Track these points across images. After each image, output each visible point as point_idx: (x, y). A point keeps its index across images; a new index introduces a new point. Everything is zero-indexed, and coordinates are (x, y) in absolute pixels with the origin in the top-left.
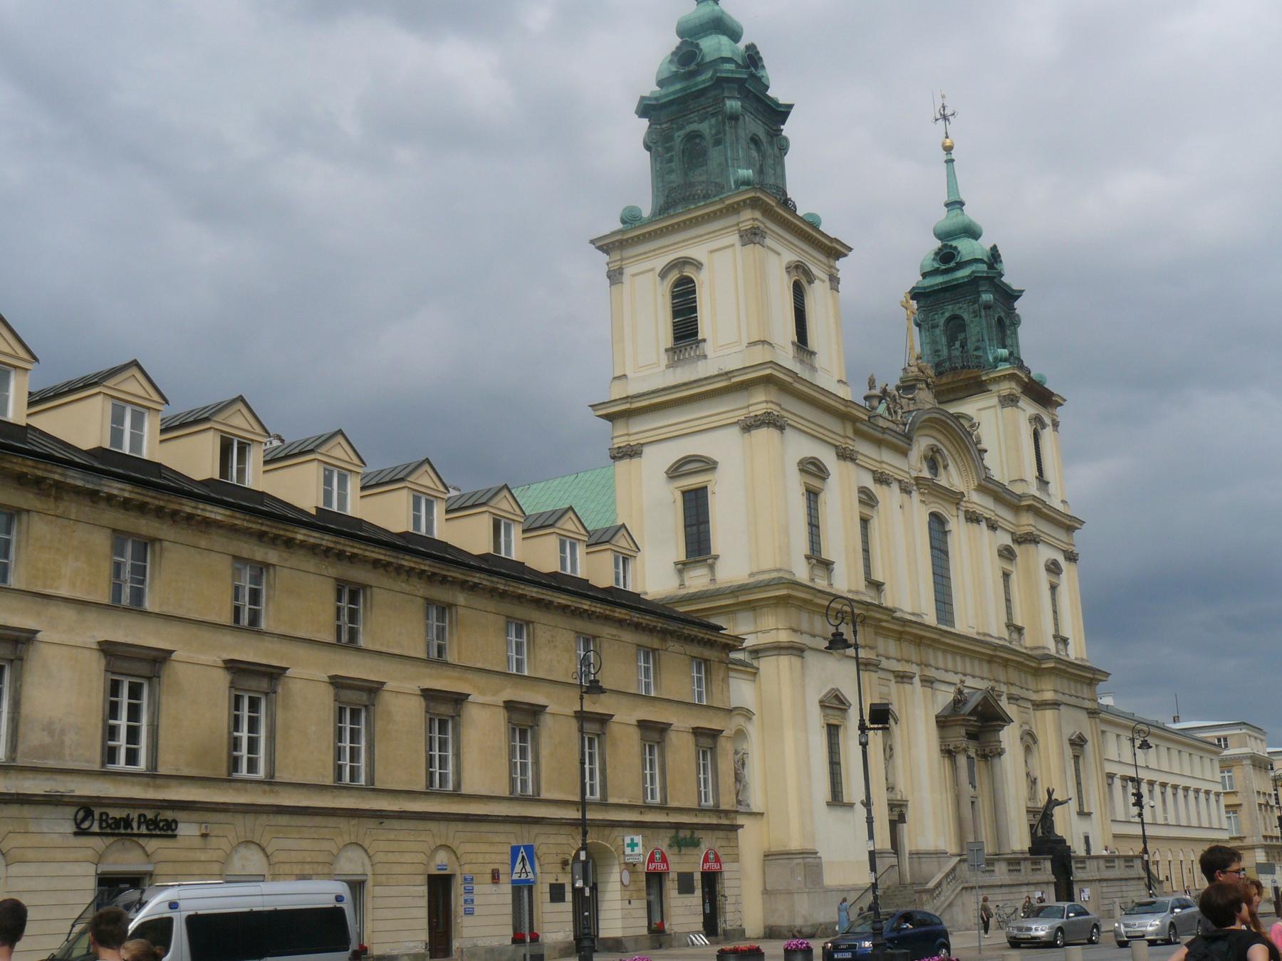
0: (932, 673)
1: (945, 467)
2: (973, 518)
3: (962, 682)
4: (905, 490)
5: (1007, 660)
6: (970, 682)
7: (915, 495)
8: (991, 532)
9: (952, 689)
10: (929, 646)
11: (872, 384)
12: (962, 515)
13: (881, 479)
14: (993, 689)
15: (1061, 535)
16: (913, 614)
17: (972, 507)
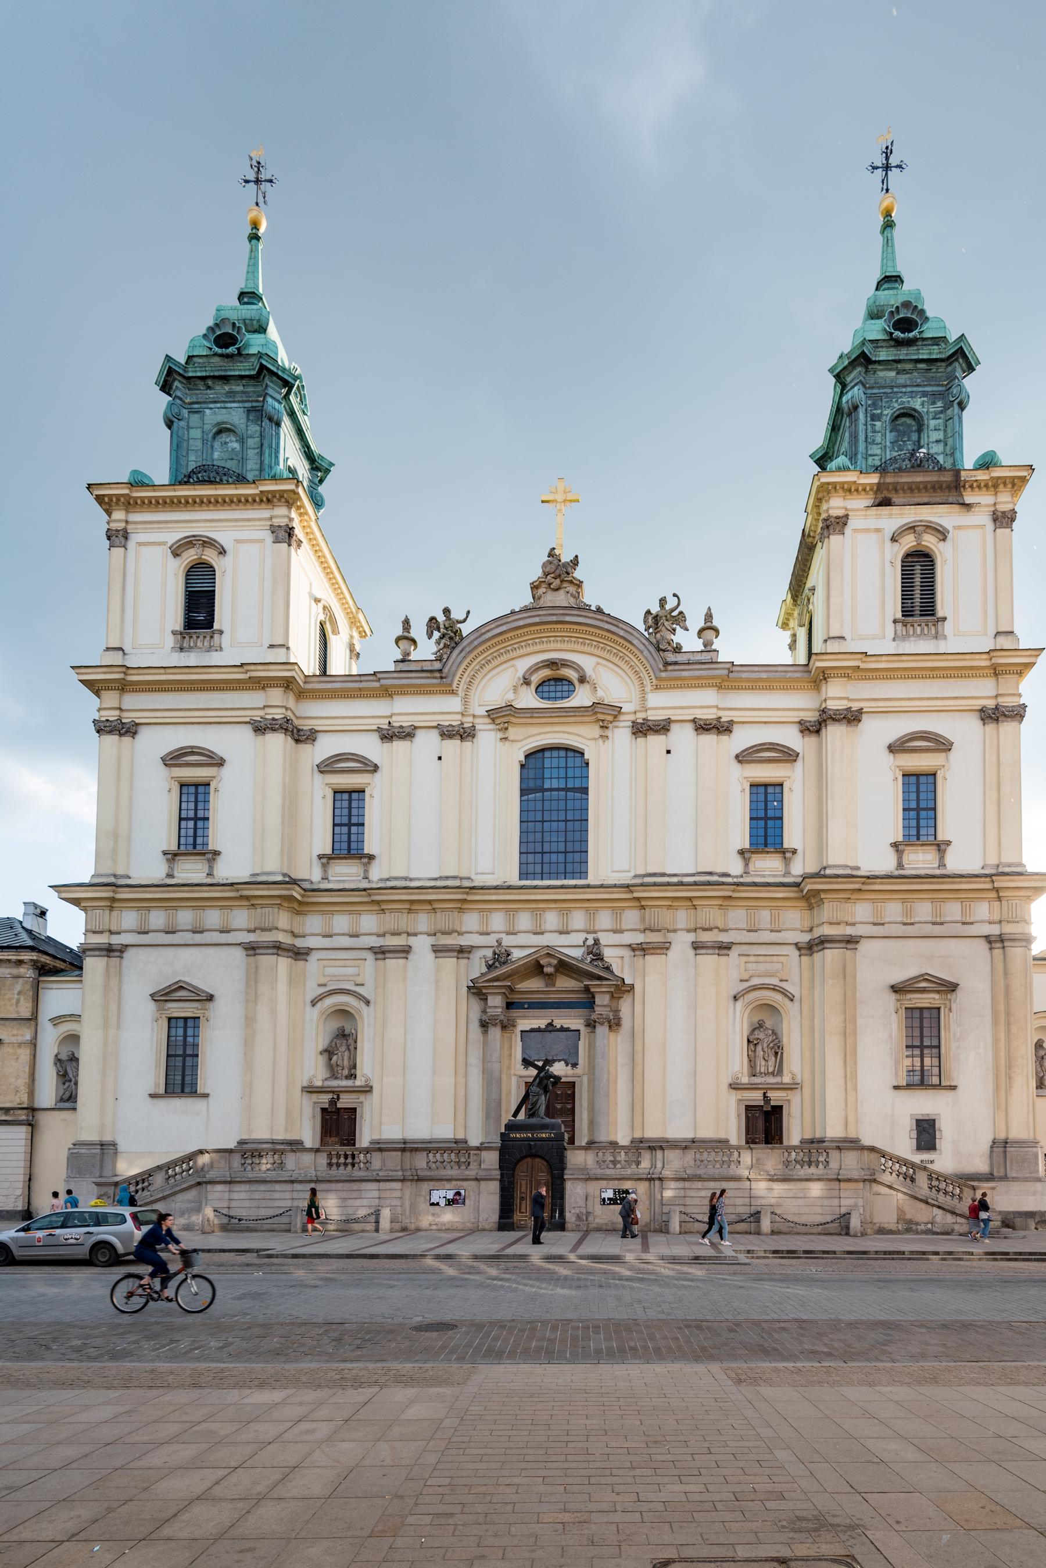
0: (465, 941)
1: (582, 680)
2: (642, 729)
3: (499, 942)
4: (447, 733)
5: (690, 899)
6: (507, 941)
7: (487, 737)
8: (709, 739)
9: (489, 953)
10: (461, 910)
11: (406, 624)
12: (621, 734)
13: (389, 735)
14: (597, 942)
15: (983, 691)
16: (440, 878)
17: (640, 717)
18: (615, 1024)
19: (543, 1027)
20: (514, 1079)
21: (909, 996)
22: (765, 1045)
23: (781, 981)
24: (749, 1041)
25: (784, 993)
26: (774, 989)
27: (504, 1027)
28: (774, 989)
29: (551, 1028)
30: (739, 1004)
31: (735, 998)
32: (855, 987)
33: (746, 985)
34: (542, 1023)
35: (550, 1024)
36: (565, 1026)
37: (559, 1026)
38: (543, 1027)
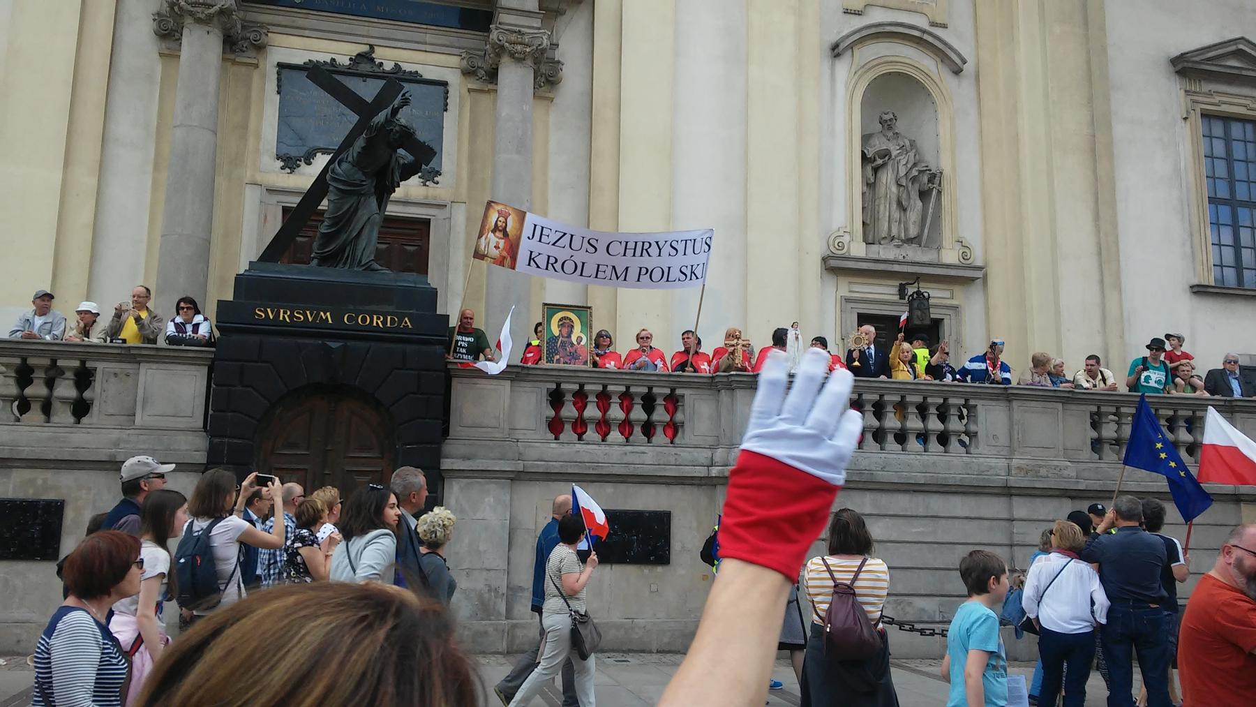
18: (547, 77)
19: (344, 61)
20: (251, 197)
21: (1207, 87)
22: (902, 172)
23: (933, 24)
24: (863, 154)
25: (941, 52)
26: (919, 40)
27: (230, 44)
28: (919, 40)
29: (365, 67)
30: (843, 68)
31: (836, 51)
32: (1104, 49)
33: (858, 23)
34: (341, 52)
35: (366, 57)
36: (407, 67)
37: (388, 66)
38: (344, 61)
